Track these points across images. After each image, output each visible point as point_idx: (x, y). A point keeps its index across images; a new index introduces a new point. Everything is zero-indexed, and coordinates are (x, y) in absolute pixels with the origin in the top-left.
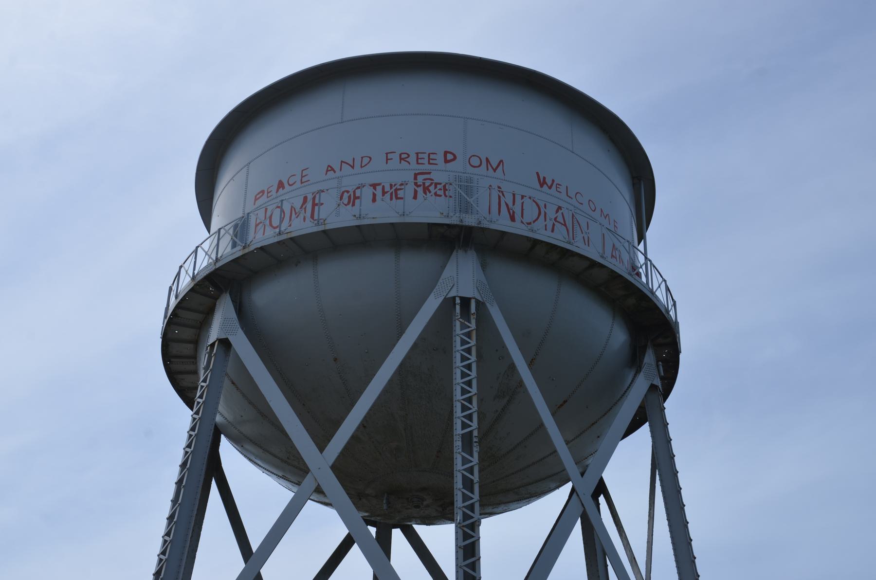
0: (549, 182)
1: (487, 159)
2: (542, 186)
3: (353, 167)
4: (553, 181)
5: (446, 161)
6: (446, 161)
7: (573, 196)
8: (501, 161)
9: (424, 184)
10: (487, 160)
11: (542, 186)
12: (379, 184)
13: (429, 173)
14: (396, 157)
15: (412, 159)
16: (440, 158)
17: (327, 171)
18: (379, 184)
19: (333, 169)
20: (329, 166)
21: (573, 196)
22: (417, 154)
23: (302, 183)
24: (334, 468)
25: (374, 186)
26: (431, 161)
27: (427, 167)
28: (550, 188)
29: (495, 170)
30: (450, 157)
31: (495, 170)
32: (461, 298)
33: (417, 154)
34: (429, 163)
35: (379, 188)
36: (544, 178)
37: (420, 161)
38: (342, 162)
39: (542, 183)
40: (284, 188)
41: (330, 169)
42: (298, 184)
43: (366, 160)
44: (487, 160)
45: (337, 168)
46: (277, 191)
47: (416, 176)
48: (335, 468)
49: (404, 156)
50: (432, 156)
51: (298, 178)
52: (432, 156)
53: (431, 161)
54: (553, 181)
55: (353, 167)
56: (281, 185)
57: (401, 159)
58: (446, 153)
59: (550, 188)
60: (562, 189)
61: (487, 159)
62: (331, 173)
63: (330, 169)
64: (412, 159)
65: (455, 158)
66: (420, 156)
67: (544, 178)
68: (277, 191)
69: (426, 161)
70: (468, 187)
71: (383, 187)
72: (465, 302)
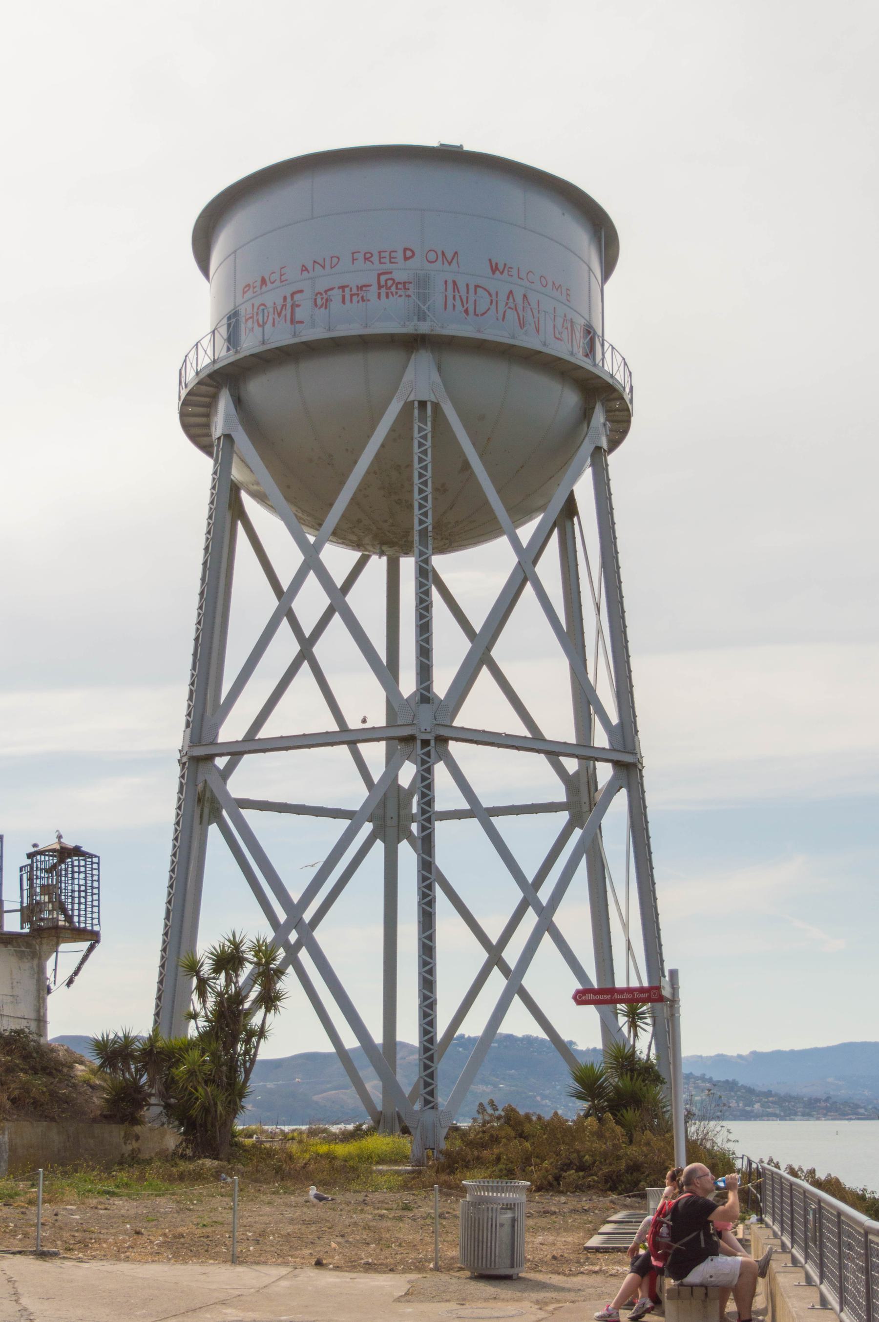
0: (501, 267)
2: (494, 272)
4: (505, 265)
5: (406, 259)
6: (406, 259)
8: (456, 253)
9: (386, 283)
11: (494, 272)
12: (347, 286)
13: (391, 273)
14: (360, 257)
15: (375, 258)
16: (400, 255)
17: (302, 271)
18: (347, 286)
19: (306, 270)
22: (380, 252)
25: (343, 288)
27: (388, 266)
28: (502, 273)
29: (450, 263)
30: (409, 254)
31: (450, 263)
33: (380, 252)
35: (347, 290)
36: (497, 264)
37: (382, 260)
38: (315, 262)
39: (494, 269)
41: (304, 269)
42: (278, 283)
43: (335, 260)
47: (379, 275)
49: (368, 255)
51: (276, 276)
57: (366, 259)
58: (405, 250)
60: (514, 272)
63: (304, 269)
64: (375, 258)
67: (497, 264)
70: (423, 282)
71: (351, 290)
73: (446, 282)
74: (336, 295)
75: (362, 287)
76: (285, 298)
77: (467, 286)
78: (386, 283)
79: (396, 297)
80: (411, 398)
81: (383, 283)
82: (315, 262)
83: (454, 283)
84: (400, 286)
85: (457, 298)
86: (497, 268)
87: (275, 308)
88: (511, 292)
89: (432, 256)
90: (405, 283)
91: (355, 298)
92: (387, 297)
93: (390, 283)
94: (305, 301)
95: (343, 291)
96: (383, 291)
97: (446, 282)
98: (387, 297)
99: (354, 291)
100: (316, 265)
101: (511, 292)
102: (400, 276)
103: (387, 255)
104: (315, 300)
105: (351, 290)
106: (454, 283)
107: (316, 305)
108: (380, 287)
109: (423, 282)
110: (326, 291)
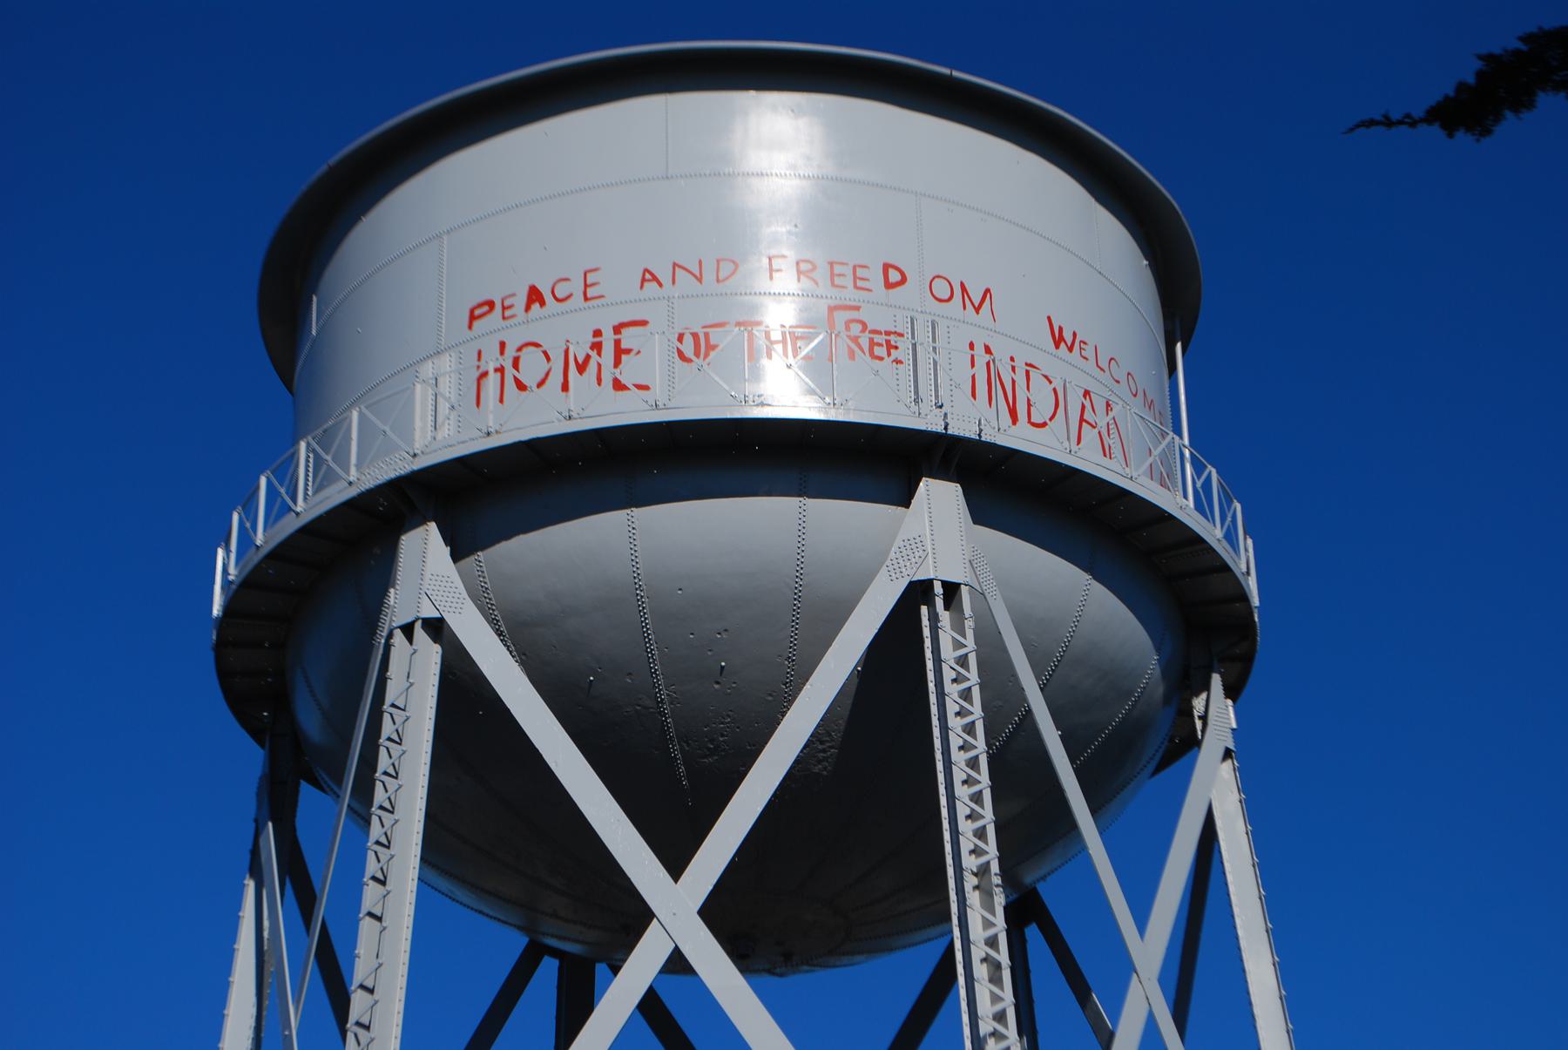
0: (1068, 337)
1: (962, 285)
2: (1057, 347)
3: (700, 280)
5: (889, 285)
6: (889, 285)
8: (988, 291)
11: (1057, 347)
13: (857, 308)
17: (644, 280)
19: (655, 278)
20: (646, 270)
23: (586, 299)
24: (706, 912)
26: (860, 283)
27: (850, 295)
28: (1071, 349)
29: (977, 310)
30: (894, 276)
31: (977, 310)
32: (945, 584)
33: (831, 264)
34: (856, 287)
36: (1061, 329)
38: (675, 265)
39: (1058, 340)
40: (543, 303)
41: (649, 277)
45: (665, 277)
46: (528, 309)
47: (832, 309)
48: (709, 913)
51: (577, 287)
52: (860, 272)
53: (860, 283)
55: (700, 280)
56: (535, 296)
57: (799, 272)
58: (886, 267)
59: (1071, 349)
60: (1089, 352)
61: (962, 285)
62: (651, 287)
65: (904, 280)
66: (837, 269)
67: (1061, 329)
68: (528, 309)
69: (848, 281)
71: (767, 335)
72: (951, 590)
73: (972, 346)
82: (675, 265)
83: (988, 350)
86: (1061, 338)
90: (888, 333)
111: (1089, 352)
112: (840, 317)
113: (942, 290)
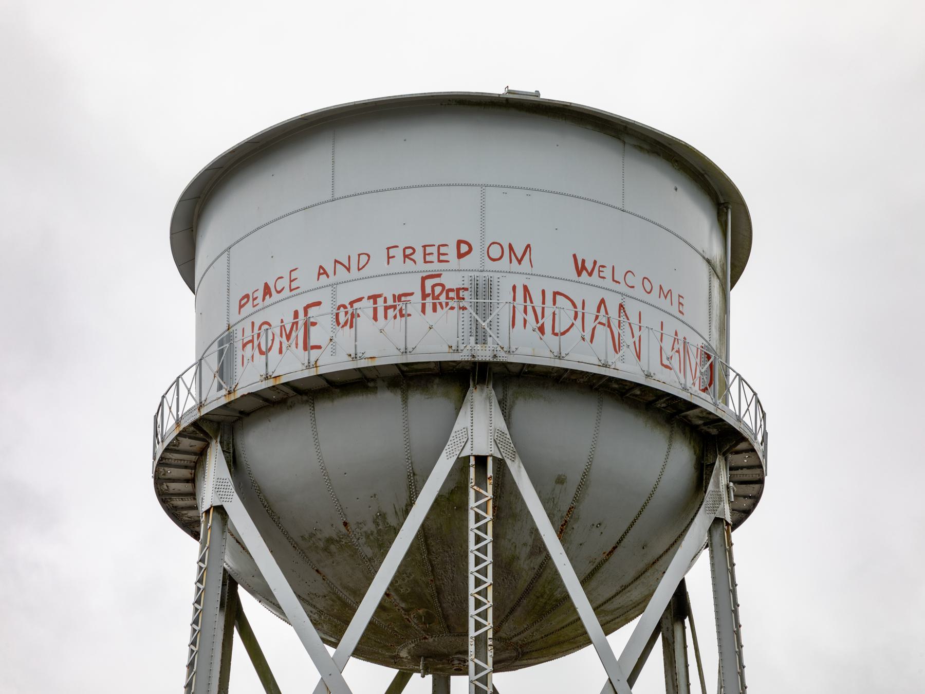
0: (589, 266)
2: (579, 274)
3: (348, 270)
4: (595, 262)
5: (460, 256)
6: (460, 256)
7: (621, 280)
8: (528, 246)
9: (433, 291)
10: (511, 248)
11: (579, 274)
12: (380, 296)
13: (439, 276)
14: (398, 253)
15: (418, 256)
16: (452, 251)
18: (380, 296)
21: (622, 281)
22: (424, 247)
25: (374, 298)
27: (436, 267)
28: (590, 274)
29: (520, 262)
30: (464, 248)
31: (520, 262)
33: (424, 247)
35: (380, 301)
36: (583, 261)
37: (428, 258)
38: (336, 261)
39: (580, 269)
41: (322, 271)
43: (364, 259)
44: (511, 248)
47: (424, 279)
49: (408, 252)
50: (443, 250)
52: (443, 250)
54: (595, 262)
55: (348, 270)
57: (405, 256)
58: (460, 242)
59: (590, 274)
60: (607, 273)
63: (322, 271)
64: (418, 256)
67: (583, 261)
70: (482, 292)
71: (385, 301)
73: (514, 288)
74: (365, 308)
75: (400, 296)
76: (296, 314)
77: (543, 292)
78: (433, 291)
79: (445, 309)
80: (465, 453)
81: (428, 290)
82: (336, 261)
83: (526, 288)
84: (451, 294)
85: (530, 309)
86: (584, 267)
87: (283, 327)
88: (602, 301)
89: (495, 252)
90: (458, 290)
91: (391, 312)
92: (435, 310)
93: (438, 290)
94: (323, 317)
95: (375, 303)
96: (429, 300)
97: (514, 288)
98: (435, 310)
99: (390, 302)
100: (338, 266)
101: (602, 301)
102: (451, 281)
103: (434, 250)
104: (337, 315)
105: (385, 301)
106: (526, 288)
107: (338, 324)
108: (424, 296)
109: (482, 292)
110: (351, 303)
111: (607, 273)
112: (429, 283)
113: (495, 252)
